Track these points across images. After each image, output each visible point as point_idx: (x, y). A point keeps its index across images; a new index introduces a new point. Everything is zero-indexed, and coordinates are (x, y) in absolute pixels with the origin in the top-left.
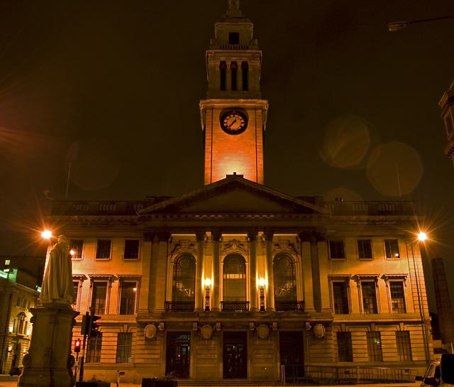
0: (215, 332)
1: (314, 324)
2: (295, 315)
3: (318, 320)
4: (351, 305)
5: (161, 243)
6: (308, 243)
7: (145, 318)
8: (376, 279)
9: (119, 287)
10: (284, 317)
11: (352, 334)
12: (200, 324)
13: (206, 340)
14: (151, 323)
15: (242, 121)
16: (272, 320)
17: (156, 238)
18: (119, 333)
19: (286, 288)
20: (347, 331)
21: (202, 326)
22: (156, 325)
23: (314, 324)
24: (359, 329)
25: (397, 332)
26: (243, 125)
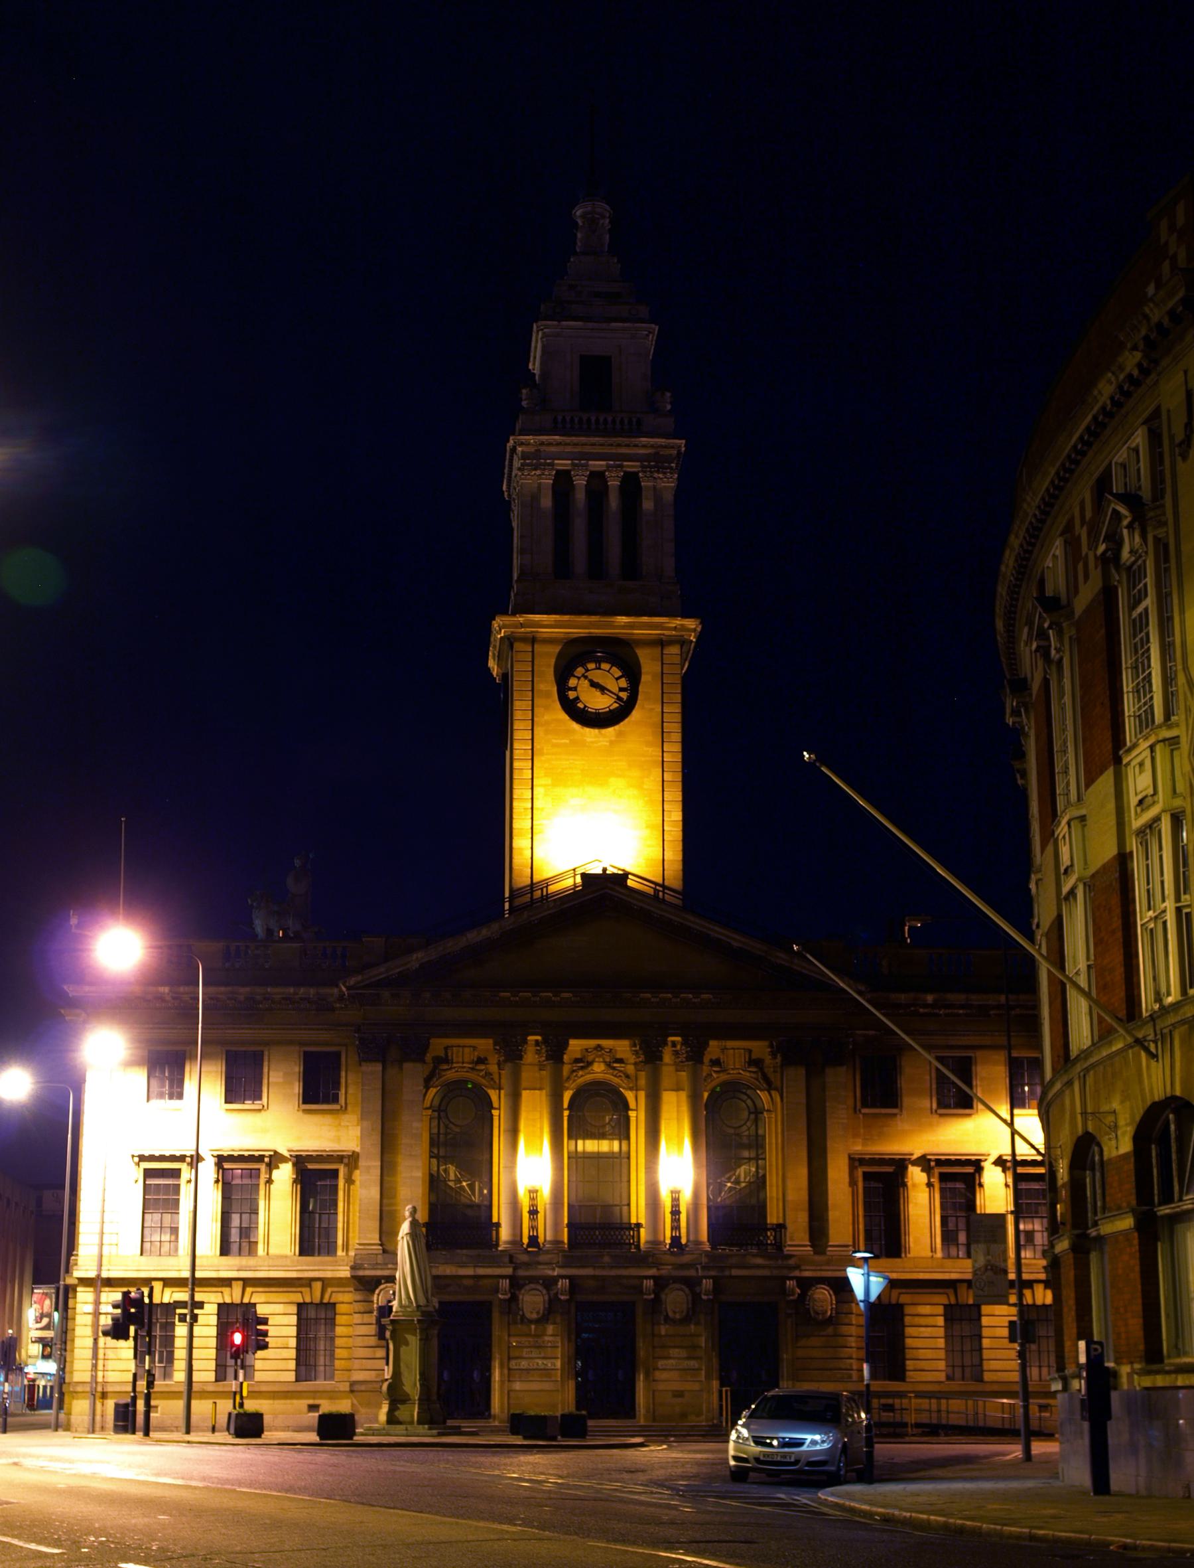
1: (806, 1284)
2: (759, 1261)
3: (819, 1274)
4: (907, 1233)
6: (802, 1071)
7: (374, 1267)
8: (977, 1165)
9: (295, 1181)
10: (731, 1267)
11: (908, 1310)
13: (531, 1321)
15: (623, 683)
16: (700, 1273)
18: (300, 1306)
19: (737, 1182)
20: (894, 1301)
23: (806, 1284)
26: (624, 695)
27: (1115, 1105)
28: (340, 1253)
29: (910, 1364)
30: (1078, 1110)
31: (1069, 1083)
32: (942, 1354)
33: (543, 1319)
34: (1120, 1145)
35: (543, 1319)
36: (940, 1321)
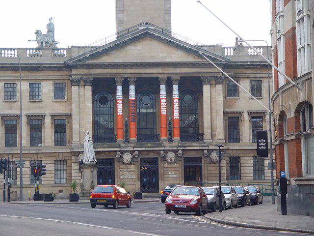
0: (133, 158)
10: (187, 146)
11: (242, 158)
12: (122, 152)
16: (178, 149)
17: (82, 83)
19: (189, 121)
21: (123, 154)
24: (246, 155)
27: (290, 103)
29: (242, 175)
30: (281, 104)
31: (278, 96)
32: (252, 172)
33: (130, 163)
34: (291, 115)
35: (130, 163)
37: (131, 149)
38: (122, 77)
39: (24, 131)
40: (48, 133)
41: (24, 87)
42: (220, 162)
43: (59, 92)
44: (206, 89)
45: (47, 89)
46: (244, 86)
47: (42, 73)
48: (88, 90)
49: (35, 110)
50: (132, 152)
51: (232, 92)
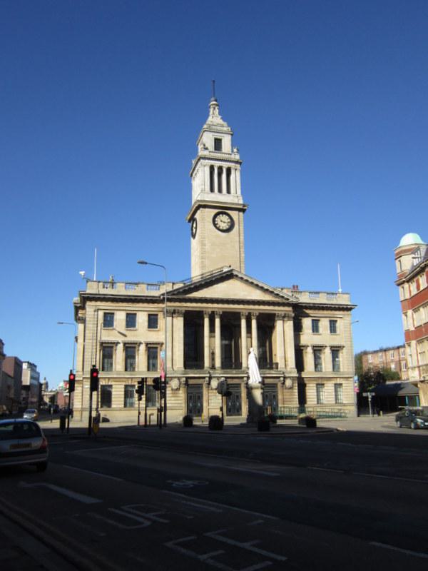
2: (274, 372)
5: (179, 318)
6: (281, 322)
14: (175, 377)
22: (179, 378)
25: (335, 384)
28: (159, 370)
36: (315, 388)
37: (218, 375)
38: (210, 311)
39: (119, 356)
40: (141, 358)
41: (120, 318)
42: (291, 388)
43: (152, 322)
44: (279, 324)
45: (142, 319)
46: (307, 323)
47: (141, 305)
48: (179, 322)
49: (132, 337)
50: (218, 378)
51: (298, 328)
